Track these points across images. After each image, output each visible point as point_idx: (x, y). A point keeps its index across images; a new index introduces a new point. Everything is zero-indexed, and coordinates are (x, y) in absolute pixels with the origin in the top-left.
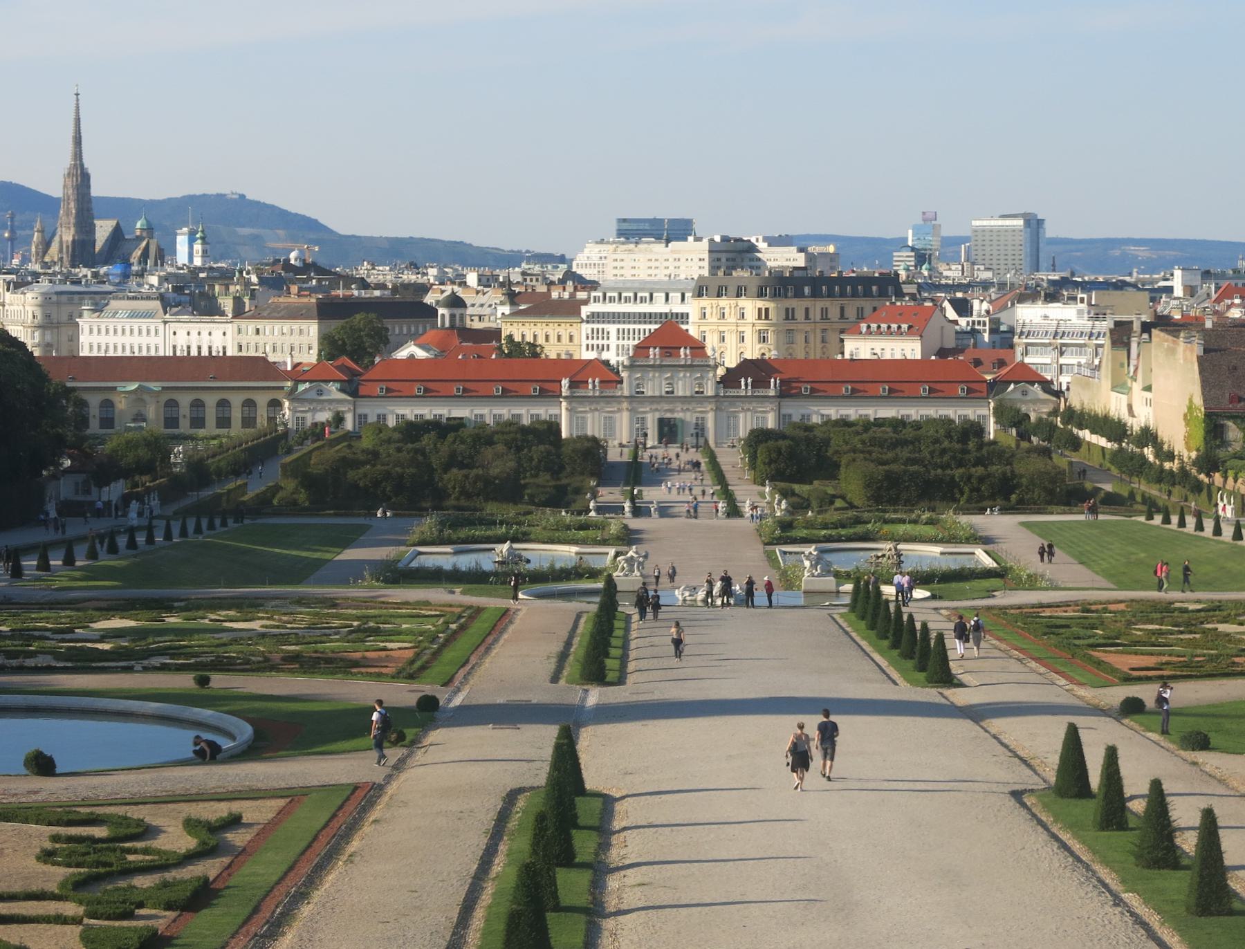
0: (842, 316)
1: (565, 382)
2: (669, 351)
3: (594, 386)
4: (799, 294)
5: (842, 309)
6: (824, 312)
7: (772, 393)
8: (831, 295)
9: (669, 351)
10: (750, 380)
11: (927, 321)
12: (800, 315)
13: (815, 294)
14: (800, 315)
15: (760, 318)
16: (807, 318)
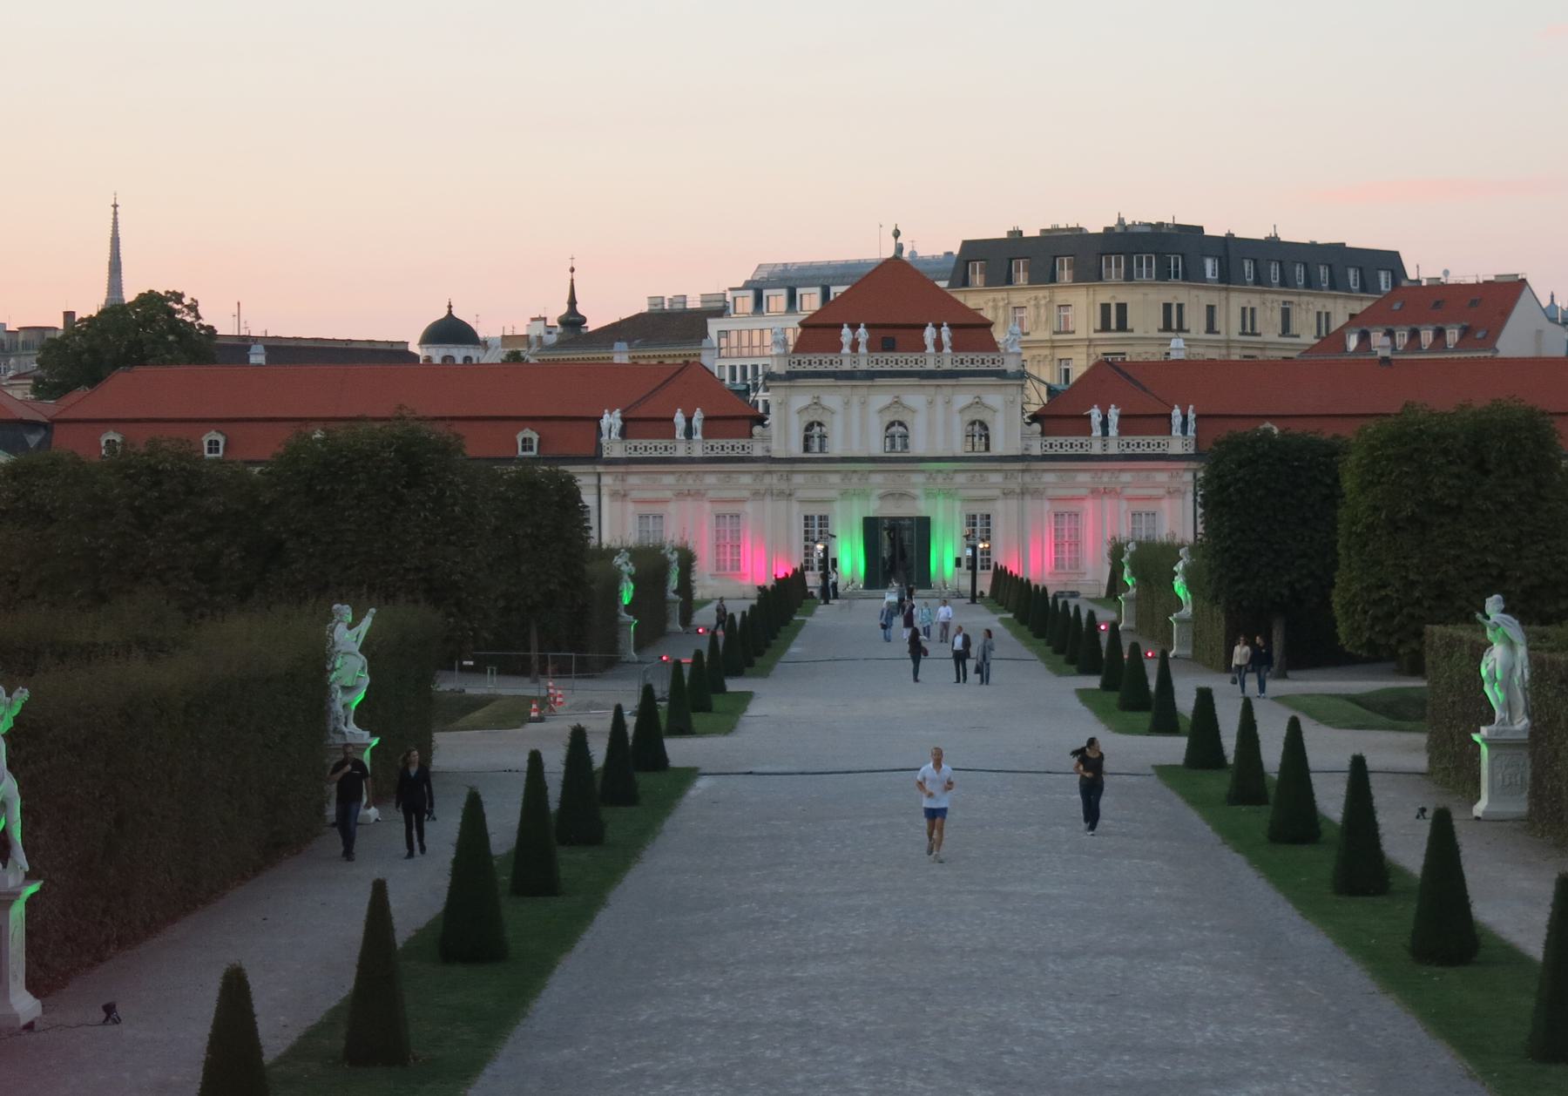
0: (1286, 330)
1: (611, 421)
2: (893, 335)
3: (689, 432)
4: (1192, 275)
5: (1286, 314)
6: (1248, 315)
7: (1177, 443)
8: (1260, 280)
9: (893, 335)
10: (1114, 414)
11: (1505, 314)
12: (1195, 321)
13: (1228, 277)
14: (1195, 321)
15: (1105, 327)
16: (1211, 329)
